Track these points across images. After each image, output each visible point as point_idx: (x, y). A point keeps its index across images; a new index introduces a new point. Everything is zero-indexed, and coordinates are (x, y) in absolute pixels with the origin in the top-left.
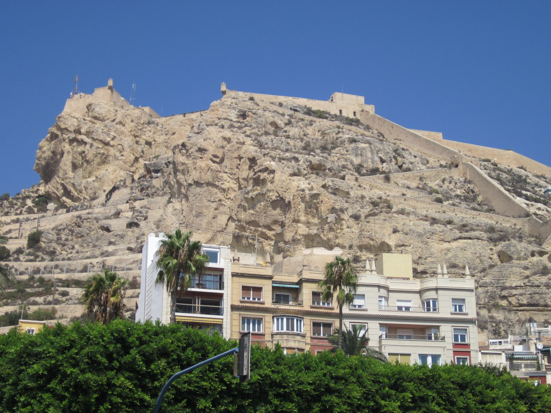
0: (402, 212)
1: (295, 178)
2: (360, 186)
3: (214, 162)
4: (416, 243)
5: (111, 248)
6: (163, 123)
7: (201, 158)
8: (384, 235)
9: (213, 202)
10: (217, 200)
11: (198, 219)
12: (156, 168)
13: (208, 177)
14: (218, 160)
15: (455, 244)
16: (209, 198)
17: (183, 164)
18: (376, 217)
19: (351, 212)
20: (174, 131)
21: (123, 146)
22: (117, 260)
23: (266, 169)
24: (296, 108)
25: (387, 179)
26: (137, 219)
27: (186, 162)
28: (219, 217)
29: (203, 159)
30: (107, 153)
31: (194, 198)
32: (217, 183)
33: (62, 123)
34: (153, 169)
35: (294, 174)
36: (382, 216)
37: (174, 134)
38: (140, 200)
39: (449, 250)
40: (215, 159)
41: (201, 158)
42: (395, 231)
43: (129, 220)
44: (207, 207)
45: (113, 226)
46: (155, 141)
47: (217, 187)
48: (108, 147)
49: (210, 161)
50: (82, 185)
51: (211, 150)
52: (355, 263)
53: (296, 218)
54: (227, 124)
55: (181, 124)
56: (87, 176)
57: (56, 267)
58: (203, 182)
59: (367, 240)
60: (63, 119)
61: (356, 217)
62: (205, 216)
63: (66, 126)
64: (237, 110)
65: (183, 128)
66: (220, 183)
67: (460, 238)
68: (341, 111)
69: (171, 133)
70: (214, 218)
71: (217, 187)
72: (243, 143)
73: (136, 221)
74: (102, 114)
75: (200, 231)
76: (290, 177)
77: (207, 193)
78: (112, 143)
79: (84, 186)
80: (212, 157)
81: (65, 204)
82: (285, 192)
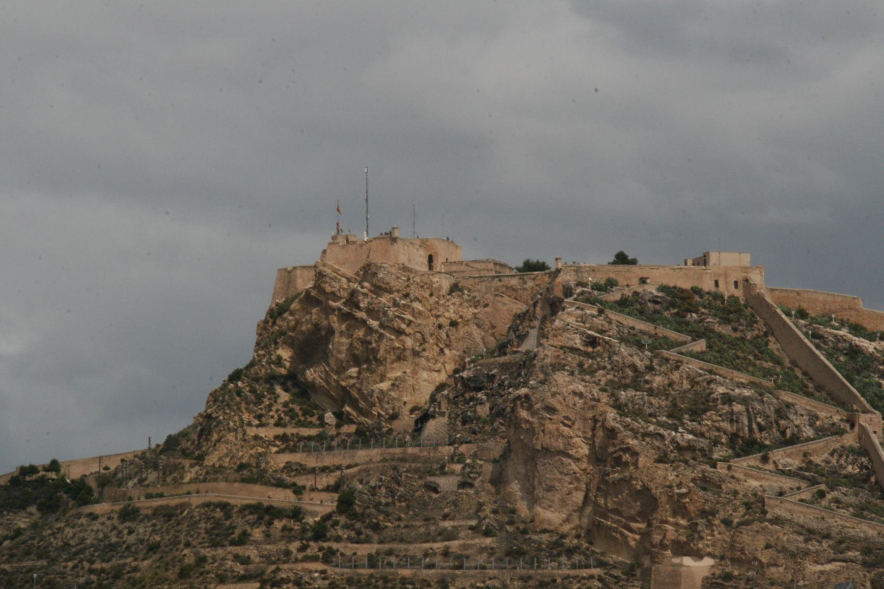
0: (777, 521)
1: (661, 465)
2: (733, 477)
3: (565, 425)
4: (789, 564)
5: (448, 524)
6: (470, 287)
7: (550, 419)
8: (756, 550)
9: (566, 475)
10: (571, 472)
11: (550, 494)
12: (478, 385)
13: (560, 444)
14: (569, 423)
15: (828, 567)
16: (561, 470)
17: (527, 421)
18: (749, 527)
19: (722, 515)
20: (486, 302)
21: (423, 335)
22: (461, 546)
23: (628, 450)
24: (656, 299)
25: (765, 459)
26: (470, 478)
27: (531, 419)
28: (574, 494)
29: (553, 421)
30: (403, 346)
31: (543, 468)
32: (570, 452)
33: (327, 285)
34: (473, 385)
35: (660, 460)
36: (756, 526)
37: (486, 305)
38: (467, 442)
39: (822, 572)
40: (566, 422)
41: (550, 419)
42: (768, 547)
43: (459, 478)
44: (560, 481)
45: (441, 486)
46: (461, 317)
47: (569, 456)
48: (403, 337)
49: (561, 425)
50: (375, 395)
51: (563, 411)
52: (726, 581)
53: (664, 518)
54: (572, 359)
55: (497, 293)
56: (378, 380)
57: (390, 553)
58: (553, 450)
59: (739, 553)
60: (328, 279)
61: (727, 523)
62: (557, 490)
63: (333, 289)
64: (585, 335)
65: (498, 299)
66: (574, 451)
67: (834, 560)
68: (717, 283)
69: (482, 304)
70: (568, 494)
71: (569, 456)
72: (598, 400)
73: (469, 481)
74: (389, 283)
75: (552, 509)
76: (655, 464)
77: (559, 463)
78: (408, 330)
79: (378, 397)
80: (563, 419)
81: (351, 417)
82: (651, 481)
